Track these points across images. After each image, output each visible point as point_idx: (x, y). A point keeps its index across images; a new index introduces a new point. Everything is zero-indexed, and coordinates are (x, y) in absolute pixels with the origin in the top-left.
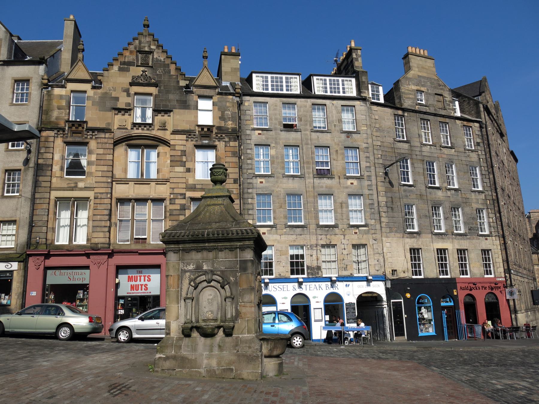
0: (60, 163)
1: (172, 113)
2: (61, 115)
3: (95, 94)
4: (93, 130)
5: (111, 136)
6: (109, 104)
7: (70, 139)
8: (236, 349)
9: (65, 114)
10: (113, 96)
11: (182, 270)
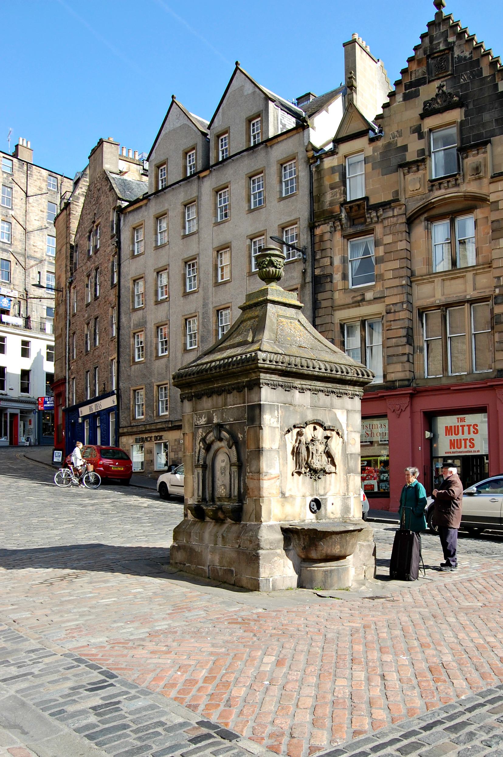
0: (341, 269)
1: (489, 146)
2: (335, 198)
3: (374, 151)
4: (376, 207)
5: (401, 211)
6: (395, 161)
7: (351, 231)
8: (237, 543)
9: (340, 194)
10: (399, 145)
11: (195, 425)
